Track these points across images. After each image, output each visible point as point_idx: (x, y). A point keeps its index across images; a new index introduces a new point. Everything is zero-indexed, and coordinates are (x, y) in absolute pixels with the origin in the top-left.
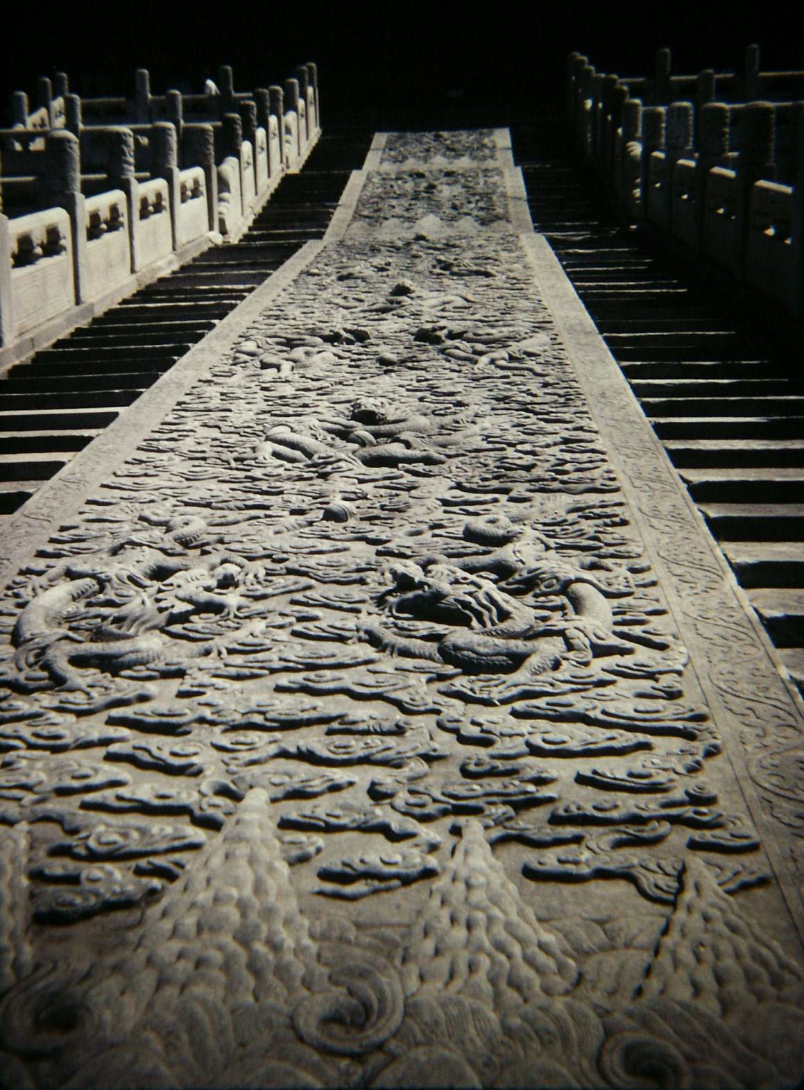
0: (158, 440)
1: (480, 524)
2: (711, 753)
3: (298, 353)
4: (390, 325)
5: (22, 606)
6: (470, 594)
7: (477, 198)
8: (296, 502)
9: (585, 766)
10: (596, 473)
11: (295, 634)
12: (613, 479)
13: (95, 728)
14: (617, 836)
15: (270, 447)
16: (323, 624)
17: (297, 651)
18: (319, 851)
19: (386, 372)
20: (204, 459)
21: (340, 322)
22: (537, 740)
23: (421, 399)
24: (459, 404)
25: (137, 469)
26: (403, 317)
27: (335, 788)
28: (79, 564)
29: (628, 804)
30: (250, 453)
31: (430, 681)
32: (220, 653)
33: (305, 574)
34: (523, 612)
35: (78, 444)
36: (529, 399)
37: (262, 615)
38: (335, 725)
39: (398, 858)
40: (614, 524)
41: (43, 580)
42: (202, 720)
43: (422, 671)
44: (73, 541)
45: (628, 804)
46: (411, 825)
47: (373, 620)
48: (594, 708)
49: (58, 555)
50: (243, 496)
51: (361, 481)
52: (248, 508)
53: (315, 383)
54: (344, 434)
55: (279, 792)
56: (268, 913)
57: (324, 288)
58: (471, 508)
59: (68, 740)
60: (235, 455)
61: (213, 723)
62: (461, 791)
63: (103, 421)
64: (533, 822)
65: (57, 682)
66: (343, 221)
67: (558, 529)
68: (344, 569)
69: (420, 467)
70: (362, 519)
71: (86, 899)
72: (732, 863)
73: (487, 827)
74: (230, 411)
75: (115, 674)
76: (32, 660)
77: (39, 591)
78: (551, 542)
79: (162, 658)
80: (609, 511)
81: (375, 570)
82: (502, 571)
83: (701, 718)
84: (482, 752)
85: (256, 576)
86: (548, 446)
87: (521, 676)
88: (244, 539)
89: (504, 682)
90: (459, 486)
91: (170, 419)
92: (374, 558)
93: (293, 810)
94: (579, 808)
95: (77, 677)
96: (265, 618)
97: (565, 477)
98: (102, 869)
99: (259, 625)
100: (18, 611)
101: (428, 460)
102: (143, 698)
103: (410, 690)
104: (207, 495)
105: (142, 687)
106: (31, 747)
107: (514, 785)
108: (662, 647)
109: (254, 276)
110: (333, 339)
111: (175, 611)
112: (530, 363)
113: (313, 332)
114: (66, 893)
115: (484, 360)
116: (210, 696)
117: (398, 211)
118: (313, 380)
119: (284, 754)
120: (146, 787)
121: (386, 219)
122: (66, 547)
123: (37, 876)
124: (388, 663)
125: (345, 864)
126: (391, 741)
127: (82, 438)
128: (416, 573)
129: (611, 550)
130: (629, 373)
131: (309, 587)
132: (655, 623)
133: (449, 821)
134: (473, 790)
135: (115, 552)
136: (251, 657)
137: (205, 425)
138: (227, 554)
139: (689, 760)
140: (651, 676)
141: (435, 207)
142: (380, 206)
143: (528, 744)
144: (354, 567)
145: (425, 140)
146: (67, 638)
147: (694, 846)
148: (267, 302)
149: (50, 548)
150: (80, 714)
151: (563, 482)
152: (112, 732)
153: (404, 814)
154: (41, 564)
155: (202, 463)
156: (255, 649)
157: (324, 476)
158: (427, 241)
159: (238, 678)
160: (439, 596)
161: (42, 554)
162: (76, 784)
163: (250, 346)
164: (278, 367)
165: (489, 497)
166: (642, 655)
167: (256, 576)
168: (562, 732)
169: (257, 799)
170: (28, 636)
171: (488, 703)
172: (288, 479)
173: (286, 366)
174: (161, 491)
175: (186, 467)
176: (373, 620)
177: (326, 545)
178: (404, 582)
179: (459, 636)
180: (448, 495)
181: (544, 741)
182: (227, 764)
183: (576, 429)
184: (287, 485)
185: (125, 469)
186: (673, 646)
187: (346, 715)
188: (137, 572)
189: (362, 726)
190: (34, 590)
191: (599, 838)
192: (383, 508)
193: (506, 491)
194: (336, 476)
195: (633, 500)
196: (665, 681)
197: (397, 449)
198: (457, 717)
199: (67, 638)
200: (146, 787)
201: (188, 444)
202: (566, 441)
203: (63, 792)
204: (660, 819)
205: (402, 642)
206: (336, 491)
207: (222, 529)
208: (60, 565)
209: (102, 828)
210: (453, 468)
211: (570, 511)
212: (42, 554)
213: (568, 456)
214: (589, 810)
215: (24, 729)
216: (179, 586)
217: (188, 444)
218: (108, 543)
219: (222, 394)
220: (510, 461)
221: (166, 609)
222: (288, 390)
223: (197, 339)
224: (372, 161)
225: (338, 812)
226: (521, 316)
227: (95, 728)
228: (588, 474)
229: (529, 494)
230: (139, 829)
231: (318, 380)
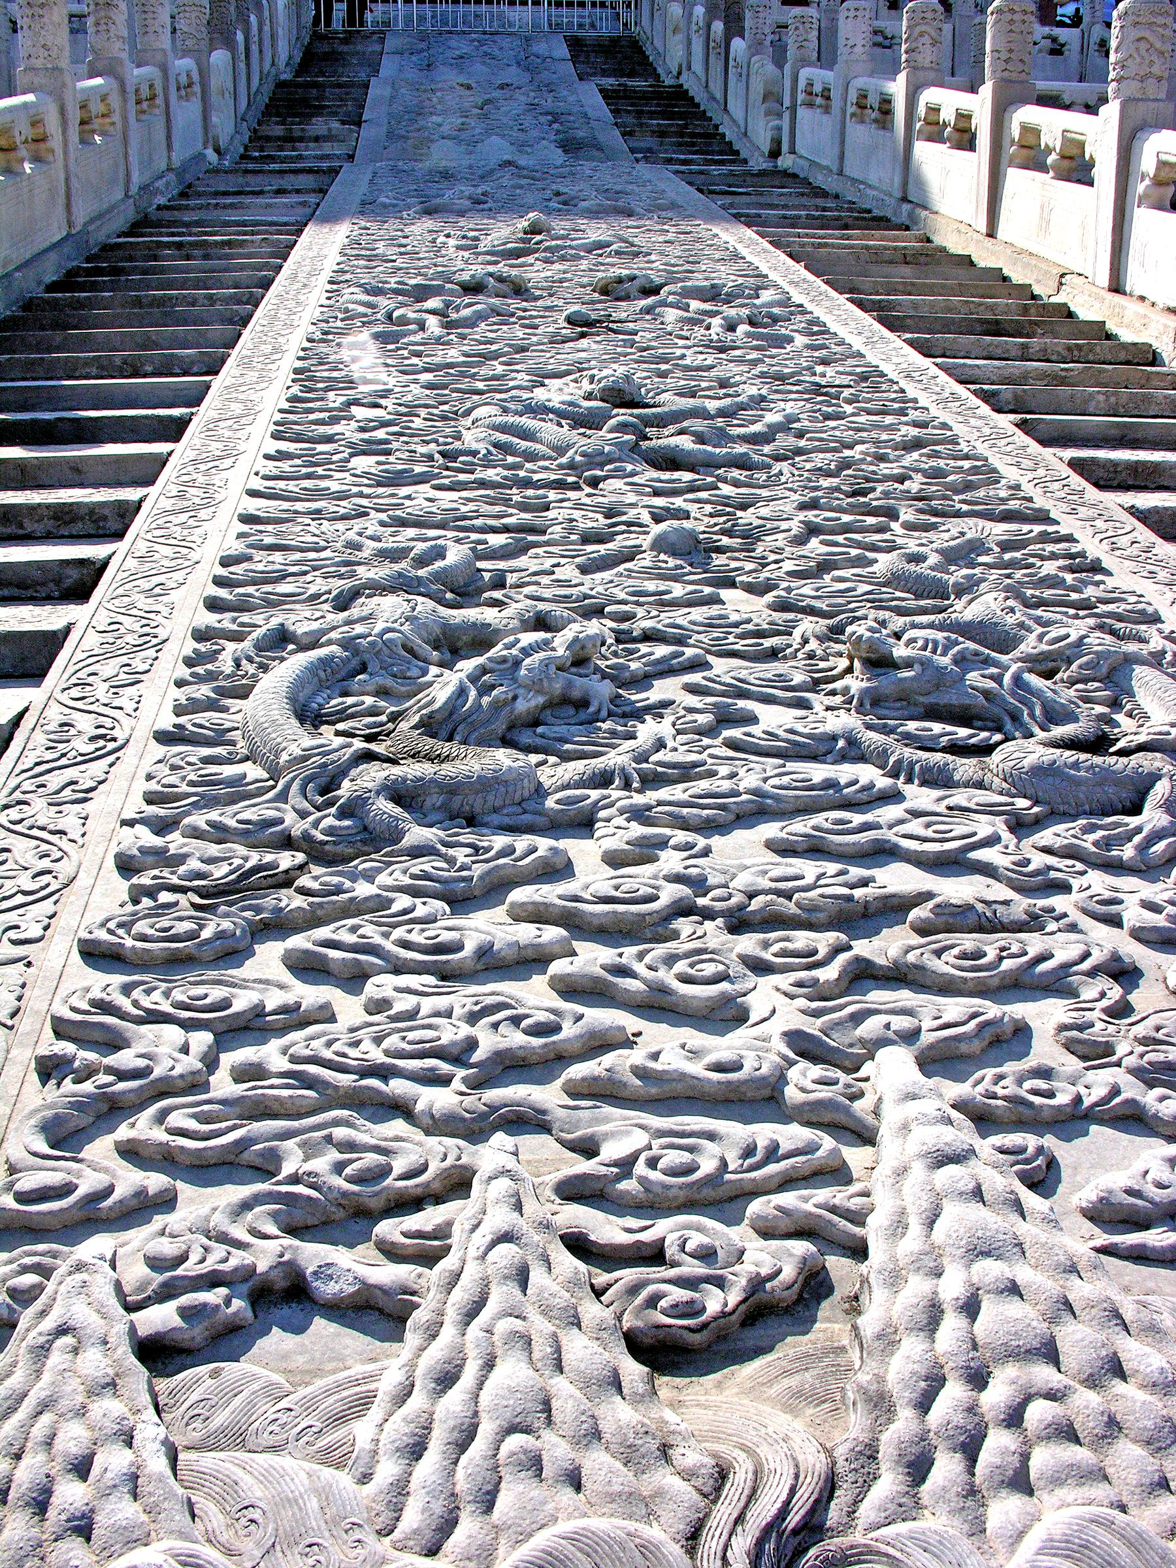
6: (991, 677)
11: (732, 744)
19: (583, 335)
24: (723, 383)
25: (286, 466)
61: (707, 914)
101: (742, 463)
111: (521, 706)
115: (716, 322)
117: (445, 129)
121: (432, 141)
125: (1130, 1192)
135: (343, 603)
142: (422, 123)
145: (453, 43)
164: (422, 327)
173: (432, 322)
184: (552, 495)
194: (617, 484)
221: (505, 703)
222: (454, 355)
224: (388, 67)
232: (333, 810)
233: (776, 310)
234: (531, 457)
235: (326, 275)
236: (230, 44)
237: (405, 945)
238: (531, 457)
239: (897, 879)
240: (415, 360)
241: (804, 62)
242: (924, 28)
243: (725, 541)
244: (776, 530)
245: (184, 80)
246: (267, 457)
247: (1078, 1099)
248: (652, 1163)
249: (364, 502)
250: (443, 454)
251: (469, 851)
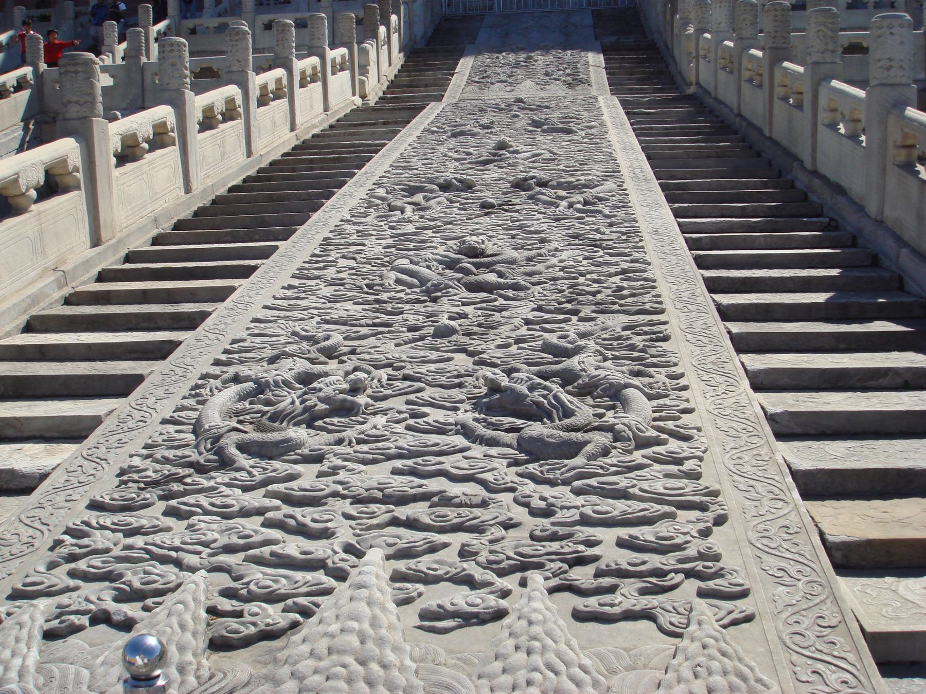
0: (307, 269)
1: (553, 339)
2: (720, 521)
3: (419, 198)
4: (493, 173)
5: (202, 403)
7: (565, 66)
8: (412, 320)
9: (624, 532)
10: (647, 298)
11: (409, 428)
12: (661, 303)
13: (255, 499)
14: (644, 585)
15: (393, 275)
16: (429, 419)
17: (408, 441)
19: (487, 214)
20: (343, 285)
21: (450, 173)
22: (588, 511)
23: (513, 237)
24: (543, 241)
25: (289, 293)
26: (502, 168)
28: (244, 370)
29: (655, 561)
30: (378, 281)
31: (509, 466)
32: (349, 444)
33: (419, 380)
34: (584, 411)
35: (246, 272)
36: (598, 236)
37: (384, 412)
38: (435, 499)
39: (479, 601)
40: (657, 340)
41: (218, 383)
42: (335, 494)
43: (503, 456)
44: (241, 352)
45: (655, 561)
46: (490, 576)
47: (466, 415)
48: (634, 486)
49: (228, 363)
50: (371, 315)
51: (464, 304)
52: (375, 325)
53: (432, 223)
54: (451, 265)
55: (391, 551)
56: (381, 642)
57: (441, 143)
58: (547, 326)
60: (367, 281)
61: (344, 497)
62: (527, 550)
63: (266, 254)
64: (583, 576)
65: (225, 463)
66: (459, 86)
67: (615, 343)
68: (448, 375)
69: (510, 293)
70: (463, 335)
71: (247, 628)
72: (728, 605)
73: (546, 579)
74: (364, 245)
75: (271, 458)
76: (209, 446)
77: (215, 391)
78: (609, 354)
79: (307, 445)
80: (655, 328)
81: (472, 376)
82: (567, 378)
83: (716, 494)
84: (546, 522)
85: (379, 381)
86: (611, 275)
87: (579, 460)
88: (372, 351)
89: (566, 466)
90: (539, 309)
91: (317, 252)
92: (471, 366)
93: (402, 565)
94: (617, 564)
95: (243, 460)
96: (386, 414)
97: (622, 302)
98: (260, 607)
99: (380, 420)
100: (200, 407)
101: (516, 287)
103: (495, 472)
104: (344, 314)
106: (206, 513)
107: (568, 547)
108: (687, 438)
109: (386, 132)
110: (446, 187)
112: (600, 207)
113: (431, 181)
114: (233, 623)
115: (564, 203)
118: (429, 220)
119: (395, 522)
120: (293, 546)
121: (492, 84)
122: (236, 356)
123: (213, 611)
124: (477, 451)
125: (439, 606)
126: (477, 512)
127: (249, 266)
128: (504, 381)
129: (655, 360)
130: (677, 214)
131: (420, 390)
132: (686, 419)
133: (518, 575)
134: (537, 550)
135: (272, 360)
136: (374, 445)
137: (343, 257)
138: (358, 363)
139: (701, 526)
140: (679, 462)
141: (530, 75)
143: (582, 515)
144: (455, 373)
146: (235, 429)
147: (702, 594)
148: (396, 155)
149: (224, 357)
150: (246, 489)
151: (621, 305)
152: (268, 502)
153: (484, 568)
154: (217, 370)
155: (342, 288)
156: (378, 439)
157: (435, 300)
158: (524, 103)
159: (364, 462)
160: (520, 397)
161: (217, 363)
162: (241, 542)
163: (381, 192)
165: (562, 317)
166: (674, 445)
167: (379, 381)
168: (608, 505)
169: (375, 556)
170: (207, 427)
171: (552, 483)
172: (407, 302)
173: (409, 209)
174: (310, 311)
175: (328, 291)
176: (466, 415)
177: (434, 355)
178: (494, 388)
179: (535, 429)
180: (530, 316)
181: (594, 512)
182: (354, 529)
183: (633, 261)
184: (407, 307)
185: (281, 293)
186: (696, 437)
187: (445, 492)
188: (288, 376)
189: (457, 500)
190: (211, 390)
191: (629, 587)
192: (480, 325)
193: (575, 312)
194: (445, 300)
195: (674, 321)
196: (688, 465)
197: (492, 277)
198: (528, 493)
199: (235, 429)
200: (293, 546)
201: (331, 273)
202: (624, 272)
203: (230, 549)
204: (676, 571)
205: (489, 433)
206: (445, 308)
207: (356, 343)
208: (232, 370)
209: (260, 576)
210: (536, 293)
211: (624, 329)
212: (217, 363)
213: (625, 284)
214: (625, 566)
215: (203, 500)
217: (331, 273)
218: (268, 353)
219: (358, 232)
220: (580, 287)
222: (411, 228)
223: (341, 185)
226: (597, 167)
227: (255, 499)
228: (639, 299)
229: (594, 315)
230: (285, 577)
231: (433, 220)
233: (600, 195)
234: (411, 286)
235: (375, 179)
237: (213, 505)
238: (411, 286)
239: (434, 485)
242: (745, 16)
243: (476, 329)
244: (506, 323)
246: (283, 288)
248: (257, 584)
250: (367, 286)
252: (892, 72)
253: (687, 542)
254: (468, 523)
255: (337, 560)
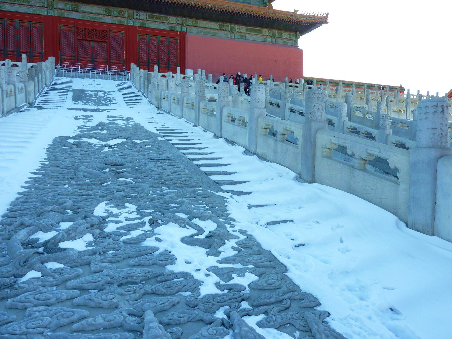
15: (81, 173)
18: (181, 334)
27: (174, 305)
32: (100, 253)
38: (159, 279)
59: (53, 300)
60: (69, 176)
61: (113, 284)
76: (22, 264)
102: (78, 276)
105: (76, 271)
116: (105, 272)
153: (205, 312)
162: (66, 321)
164: (71, 148)
169: (149, 316)
184: (94, 187)
203: (61, 327)
216: (77, 228)
225: (182, 315)
232: (26, 267)
236: (33, 80)
240: (68, 156)
241: (163, 90)
245: (20, 88)
247: (189, 317)
249: (50, 190)
251: (58, 274)
252: (259, 104)
253: (280, 284)
254: (183, 288)
255: (129, 322)
